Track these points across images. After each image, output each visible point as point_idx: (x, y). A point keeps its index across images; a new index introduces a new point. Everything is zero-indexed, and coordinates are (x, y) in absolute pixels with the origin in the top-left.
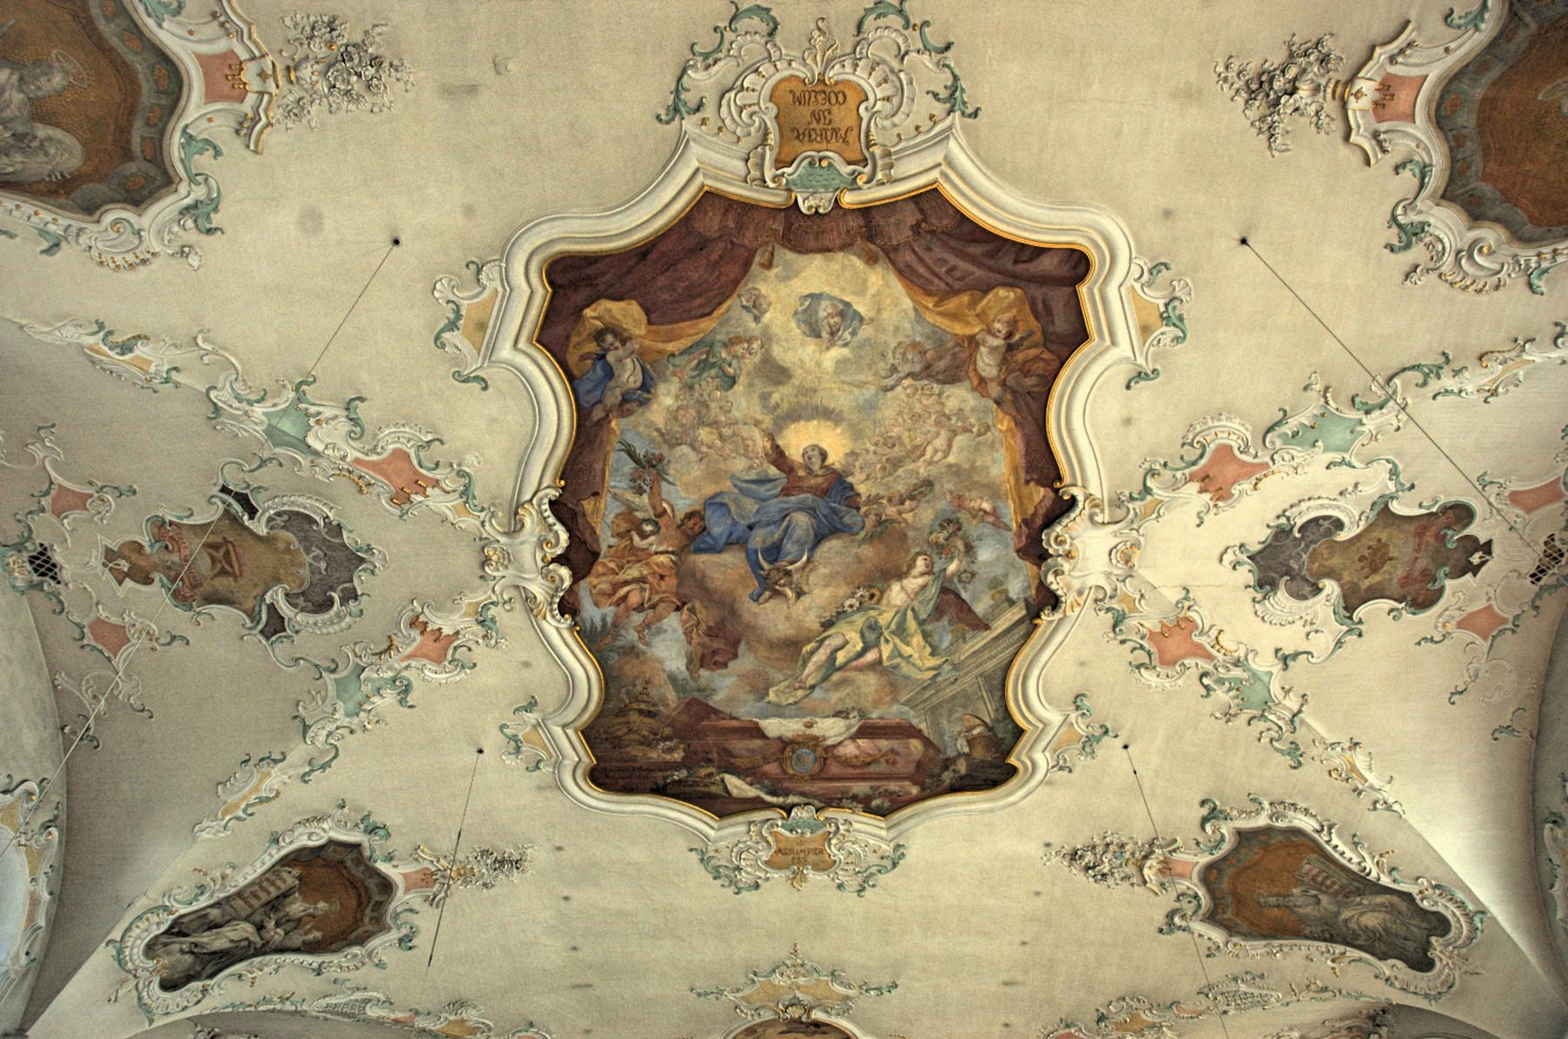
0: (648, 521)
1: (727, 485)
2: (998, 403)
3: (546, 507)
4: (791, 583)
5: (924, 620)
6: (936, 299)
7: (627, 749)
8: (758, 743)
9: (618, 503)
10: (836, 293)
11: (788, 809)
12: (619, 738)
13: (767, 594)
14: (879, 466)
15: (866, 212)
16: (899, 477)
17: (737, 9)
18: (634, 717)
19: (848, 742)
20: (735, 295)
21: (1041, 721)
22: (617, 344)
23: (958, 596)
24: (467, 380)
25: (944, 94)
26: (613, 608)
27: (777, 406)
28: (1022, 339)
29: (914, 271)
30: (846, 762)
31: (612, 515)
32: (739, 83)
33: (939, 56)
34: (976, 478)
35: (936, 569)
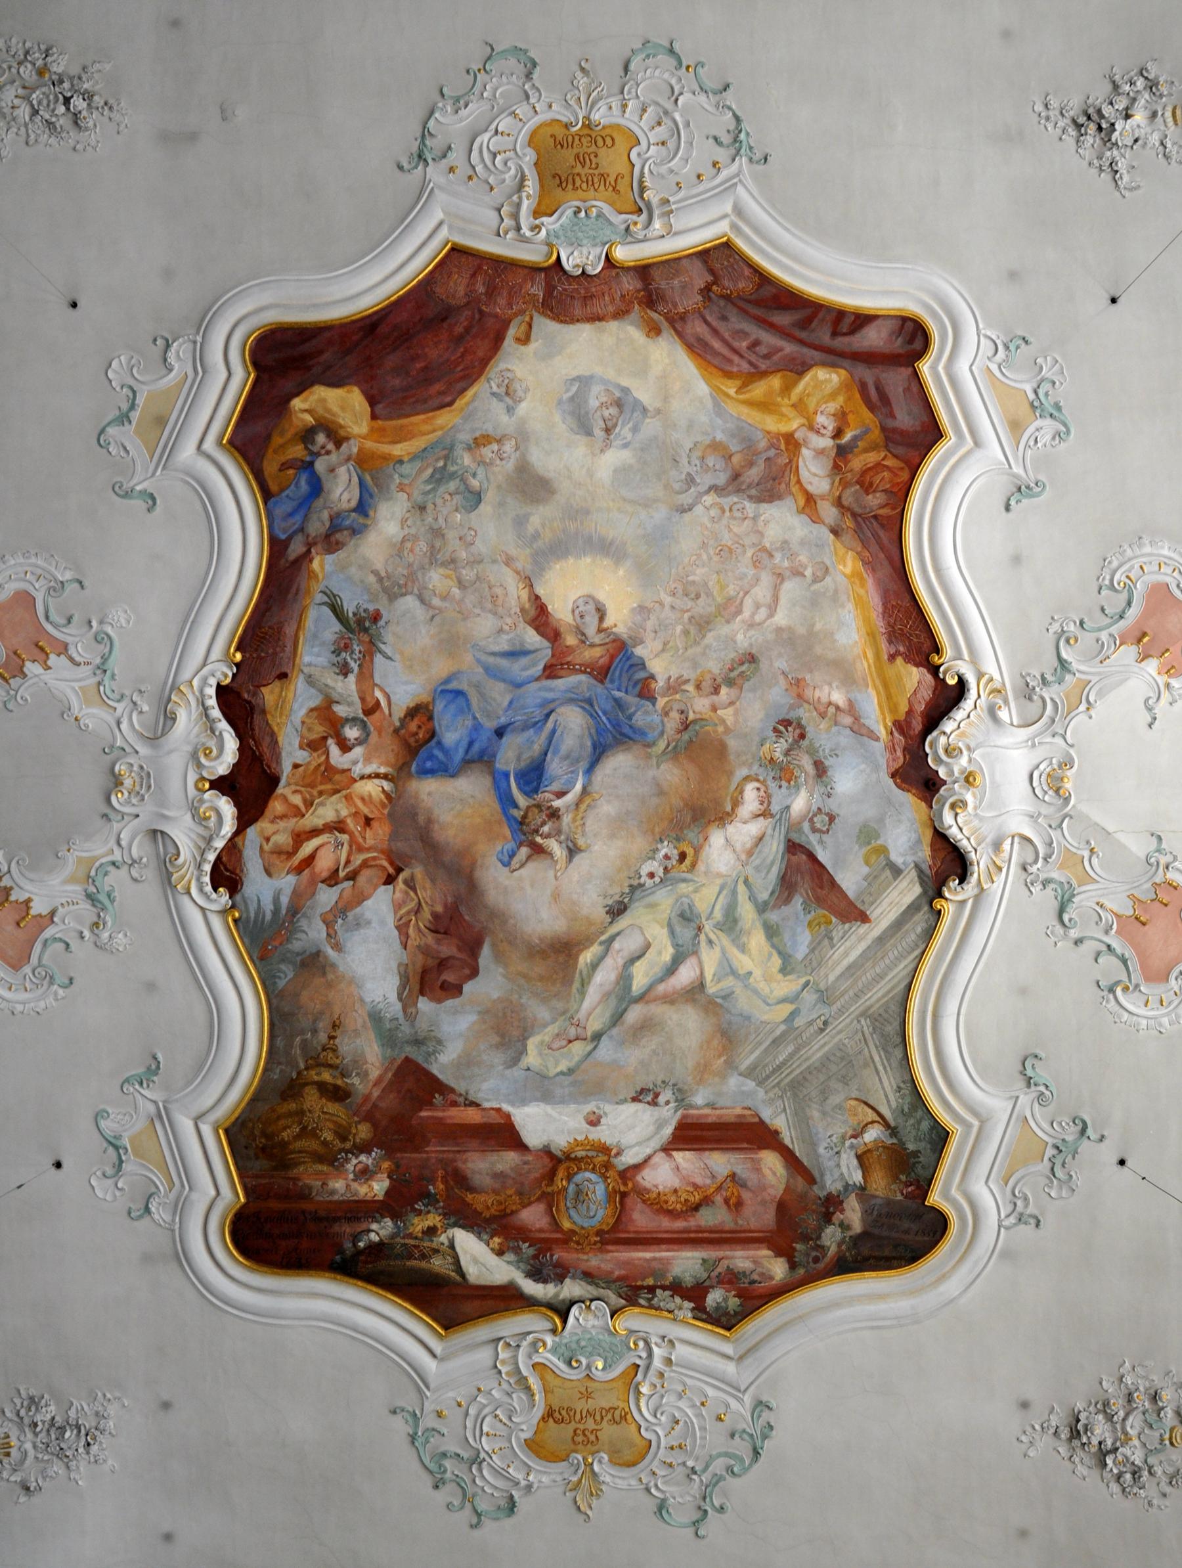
0: (354, 720)
1: (467, 659)
2: (835, 532)
3: (211, 691)
4: (559, 832)
5: (766, 903)
6: (738, 383)
7: (295, 1172)
8: (508, 1160)
9: (313, 691)
10: (610, 374)
11: (562, 1311)
12: (284, 1145)
13: (524, 851)
14: (679, 628)
15: (644, 271)
16: (708, 647)
17: (493, 49)
18: (312, 1099)
19: (660, 1158)
20: (483, 378)
21: (976, 1114)
22: (330, 446)
23: (812, 857)
24: (128, 495)
25: (726, 139)
26: (291, 879)
27: (536, 536)
28: (855, 439)
29: (705, 345)
30: (658, 1204)
31: (303, 711)
32: (493, 126)
33: (717, 97)
34: (818, 650)
35: (775, 808)
